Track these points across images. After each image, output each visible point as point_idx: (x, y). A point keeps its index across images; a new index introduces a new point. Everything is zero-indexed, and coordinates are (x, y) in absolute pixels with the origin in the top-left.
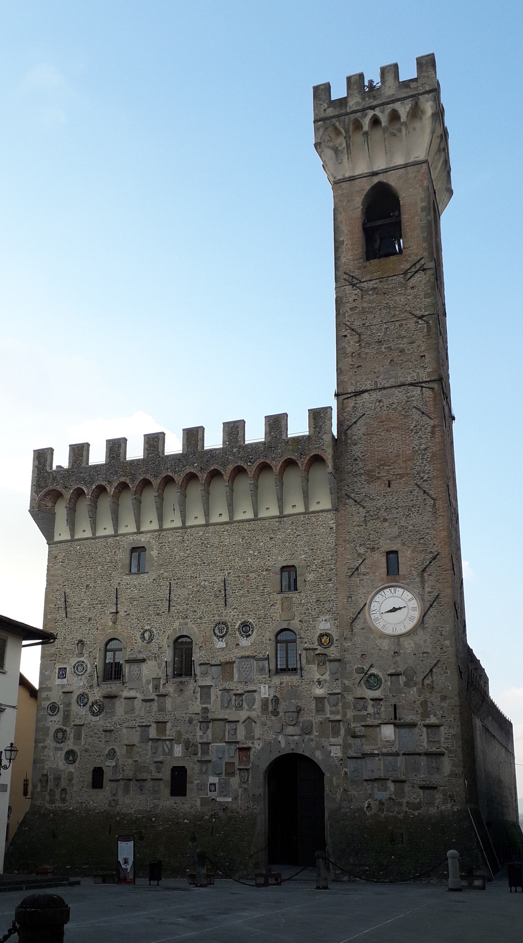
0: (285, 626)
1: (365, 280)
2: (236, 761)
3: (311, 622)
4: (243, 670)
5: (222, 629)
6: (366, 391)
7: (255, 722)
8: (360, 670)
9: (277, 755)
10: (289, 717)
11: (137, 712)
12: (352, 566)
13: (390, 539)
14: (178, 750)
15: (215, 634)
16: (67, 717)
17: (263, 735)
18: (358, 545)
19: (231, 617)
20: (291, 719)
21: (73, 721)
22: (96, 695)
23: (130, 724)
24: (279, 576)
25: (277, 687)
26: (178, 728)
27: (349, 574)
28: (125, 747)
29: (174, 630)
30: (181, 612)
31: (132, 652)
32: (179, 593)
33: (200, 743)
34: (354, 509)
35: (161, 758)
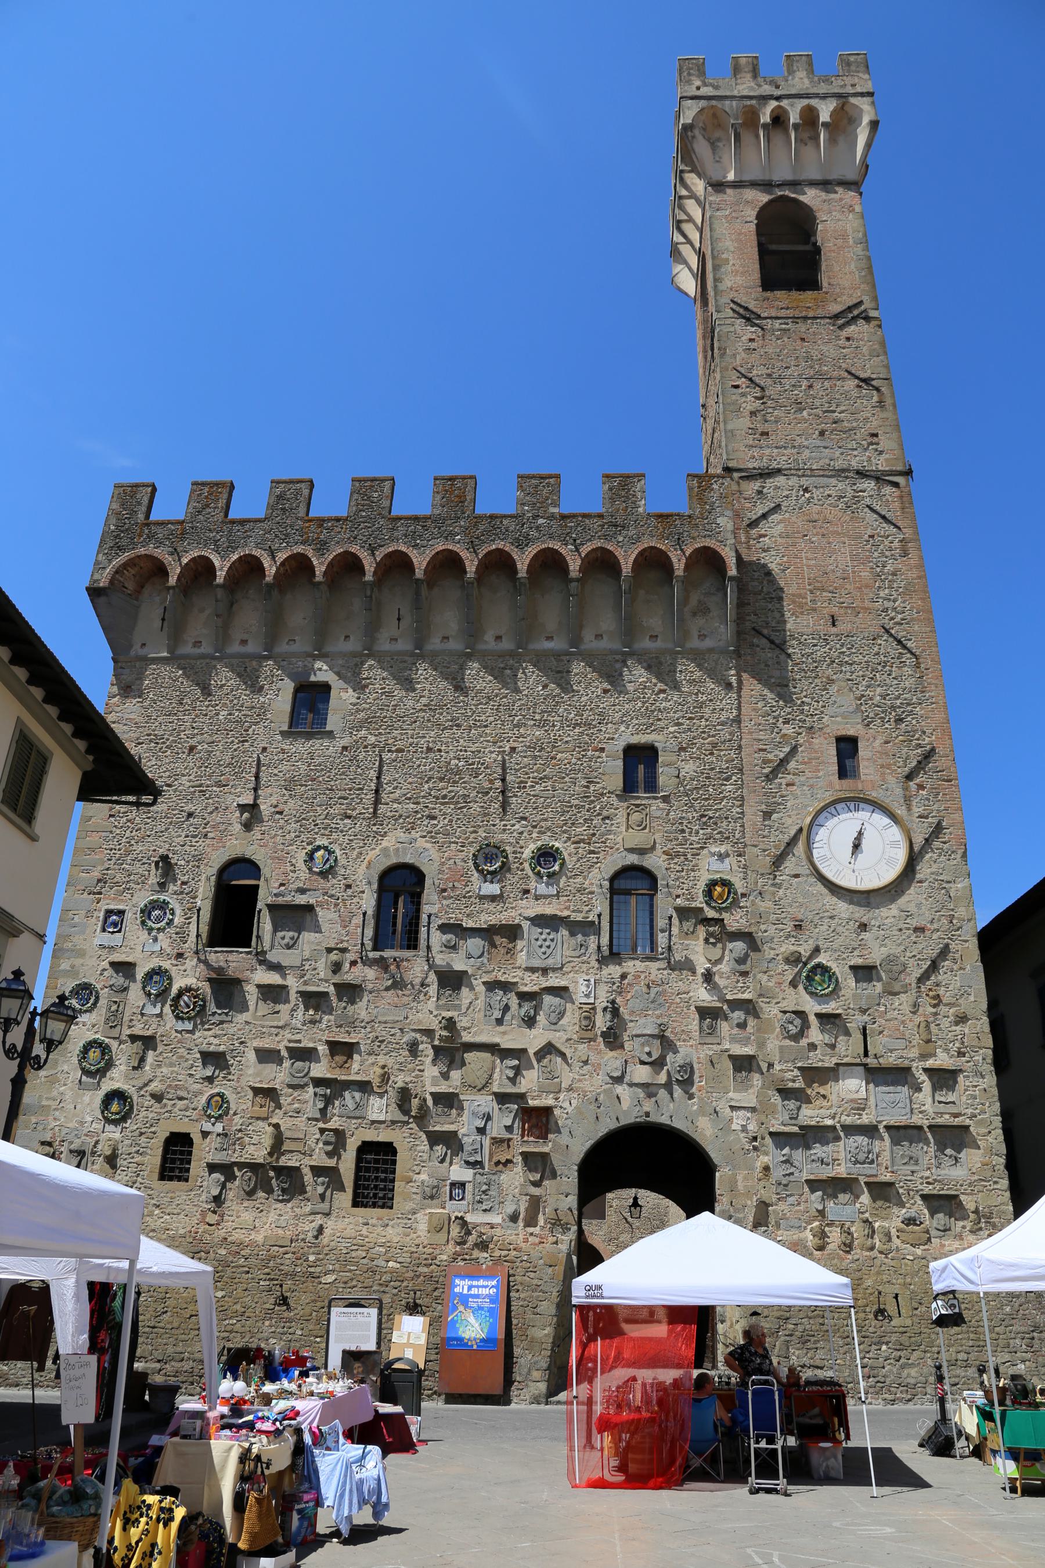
0: (633, 859)
1: (766, 315)
2: (516, 1136)
3: (689, 856)
4: (539, 943)
5: (492, 860)
7: (563, 1055)
8: (794, 959)
9: (612, 1125)
10: (643, 1045)
11: (284, 1017)
12: (770, 756)
14: (378, 1108)
15: (476, 866)
16: (114, 1019)
17: (580, 1080)
18: (781, 720)
20: (647, 1049)
21: (130, 1027)
22: (188, 976)
23: (266, 1043)
24: (620, 763)
25: (614, 983)
26: (381, 1060)
27: (767, 771)
28: (250, 1094)
29: (385, 849)
30: (401, 816)
31: (282, 888)
32: (399, 785)
33: (431, 1094)
34: (769, 655)
35: (334, 1123)
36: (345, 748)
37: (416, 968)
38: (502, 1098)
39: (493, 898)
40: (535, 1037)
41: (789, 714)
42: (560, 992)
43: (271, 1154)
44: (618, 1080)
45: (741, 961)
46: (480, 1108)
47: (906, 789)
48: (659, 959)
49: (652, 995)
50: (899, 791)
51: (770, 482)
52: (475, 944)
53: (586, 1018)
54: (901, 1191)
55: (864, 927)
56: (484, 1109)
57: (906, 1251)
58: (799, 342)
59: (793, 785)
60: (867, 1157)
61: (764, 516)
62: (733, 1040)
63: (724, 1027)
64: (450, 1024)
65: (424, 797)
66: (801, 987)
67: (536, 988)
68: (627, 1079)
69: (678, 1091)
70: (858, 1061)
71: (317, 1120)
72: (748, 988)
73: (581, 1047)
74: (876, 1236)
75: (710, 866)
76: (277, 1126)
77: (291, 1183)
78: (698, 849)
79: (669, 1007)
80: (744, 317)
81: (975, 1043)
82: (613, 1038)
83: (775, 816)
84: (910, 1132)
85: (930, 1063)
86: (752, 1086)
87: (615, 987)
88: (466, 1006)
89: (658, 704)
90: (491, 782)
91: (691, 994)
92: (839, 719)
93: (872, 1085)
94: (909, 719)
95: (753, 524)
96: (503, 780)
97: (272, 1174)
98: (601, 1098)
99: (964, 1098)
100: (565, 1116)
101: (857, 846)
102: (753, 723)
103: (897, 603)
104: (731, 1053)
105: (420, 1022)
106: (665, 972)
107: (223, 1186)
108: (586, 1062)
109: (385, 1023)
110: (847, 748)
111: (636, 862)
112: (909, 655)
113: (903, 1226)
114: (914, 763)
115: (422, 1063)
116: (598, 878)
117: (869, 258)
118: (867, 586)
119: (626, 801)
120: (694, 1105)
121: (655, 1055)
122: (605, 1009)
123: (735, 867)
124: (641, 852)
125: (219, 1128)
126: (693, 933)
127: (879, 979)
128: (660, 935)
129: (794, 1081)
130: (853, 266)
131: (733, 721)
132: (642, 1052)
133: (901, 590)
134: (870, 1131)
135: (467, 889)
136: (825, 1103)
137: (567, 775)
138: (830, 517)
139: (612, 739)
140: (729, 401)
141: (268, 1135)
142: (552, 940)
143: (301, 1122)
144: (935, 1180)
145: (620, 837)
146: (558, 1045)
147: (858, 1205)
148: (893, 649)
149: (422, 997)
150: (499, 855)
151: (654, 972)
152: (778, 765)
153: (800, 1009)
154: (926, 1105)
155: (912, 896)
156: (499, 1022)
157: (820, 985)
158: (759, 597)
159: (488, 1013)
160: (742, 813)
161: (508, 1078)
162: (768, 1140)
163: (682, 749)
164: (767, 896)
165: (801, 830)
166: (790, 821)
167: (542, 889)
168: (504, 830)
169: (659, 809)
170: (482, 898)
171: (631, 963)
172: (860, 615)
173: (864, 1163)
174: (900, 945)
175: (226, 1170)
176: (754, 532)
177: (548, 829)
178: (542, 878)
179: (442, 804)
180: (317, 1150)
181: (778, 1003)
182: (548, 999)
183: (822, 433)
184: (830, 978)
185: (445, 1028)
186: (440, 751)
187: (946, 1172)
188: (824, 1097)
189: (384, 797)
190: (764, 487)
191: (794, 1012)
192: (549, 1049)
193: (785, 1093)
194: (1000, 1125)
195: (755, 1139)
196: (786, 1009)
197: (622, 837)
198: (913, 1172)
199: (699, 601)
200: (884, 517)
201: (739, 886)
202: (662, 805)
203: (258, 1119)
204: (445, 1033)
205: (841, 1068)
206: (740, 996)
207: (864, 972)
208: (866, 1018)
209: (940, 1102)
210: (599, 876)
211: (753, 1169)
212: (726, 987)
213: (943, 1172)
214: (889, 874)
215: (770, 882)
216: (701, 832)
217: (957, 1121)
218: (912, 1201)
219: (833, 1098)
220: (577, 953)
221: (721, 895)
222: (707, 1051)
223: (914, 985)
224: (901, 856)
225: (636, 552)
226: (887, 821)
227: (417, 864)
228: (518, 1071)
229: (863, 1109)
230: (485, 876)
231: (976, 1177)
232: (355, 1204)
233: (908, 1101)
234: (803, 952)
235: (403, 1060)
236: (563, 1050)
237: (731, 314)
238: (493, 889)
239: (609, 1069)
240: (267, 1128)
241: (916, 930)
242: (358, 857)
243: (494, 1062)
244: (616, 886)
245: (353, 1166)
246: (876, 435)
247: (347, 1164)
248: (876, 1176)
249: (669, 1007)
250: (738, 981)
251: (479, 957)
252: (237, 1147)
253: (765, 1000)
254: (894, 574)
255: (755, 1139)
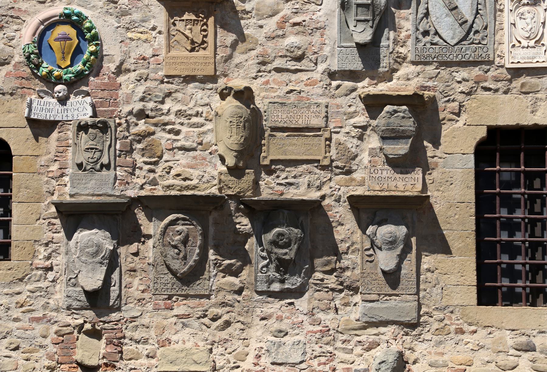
35: (405, 81)
43: (235, 172)
71: (353, 76)
76: (245, 96)
77: (298, 241)
97: (244, 223)
107: (113, 262)
125: (80, 109)
141: (223, 123)
143: (311, 82)
175: (118, 219)
180: (365, 158)
203: (189, 79)
232: (486, 296)
240: (216, 102)
245: (471, 195)
247: (451, 184)
252: (140, 160)
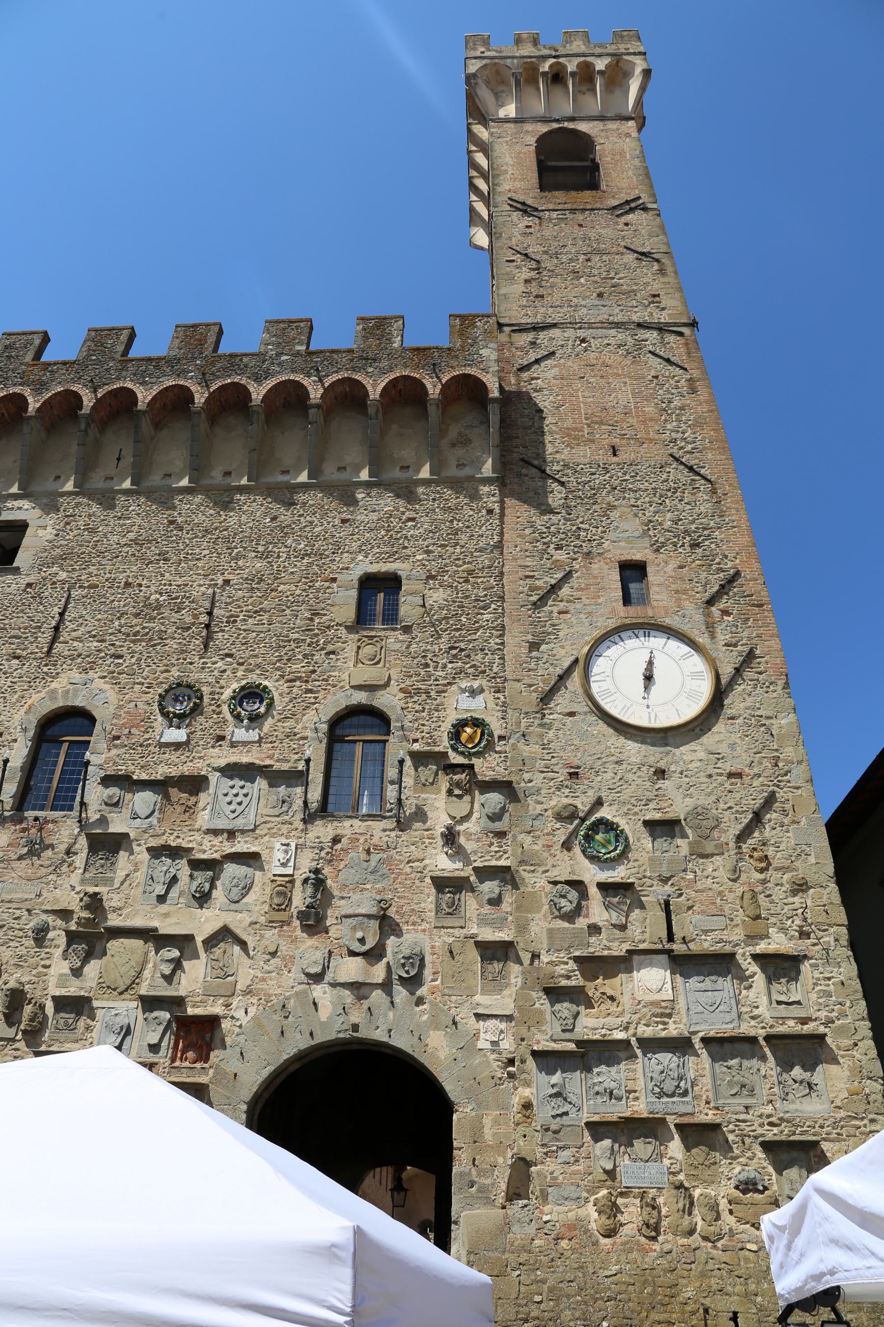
0: (360, 697)
3: (433, 694)
4: (228, 799)
5: (182, 702)
6: (554, 325)
7: (243, 944)
8: (568, 815)
10: (354, 929)
12: (539, 583)
13: (628, 540)
15: (162, 708)
17: (263, 980)
18: (552, 546)
19: (216, 673)
20: (359, 935)
24: (354, 593)
25: (322, 849)
27: (535, 598)
30: (79, 655)
32: (83, 621)
33: (54, 998)
36: (29, 585)
37: (65, 830)
38: (150, 1003)
39: (177, 746)
40: (207, 920)
41: (562, 539)
42: (251, 859)
44: (317, 978)
45: (495, 817)
46: (118, 1019)
47: (708, 615)
48: (385, 818)
49: (373, 863)
50: (699, 617)
51: (542, 335)
52: (144, 800)
53: (279, 894)
54: (731, 1137)
55: (661, 773)
56: (123, 1021)
57: (744, 1237)
58: (576, 227)
59: (566, 612)
60: (678, 1086)
61: (537, 361)
62: (483, 921)
63: (470, 904)
64: (95, 903)
65: (111, 634)
66: (577, 850)
67: (217, 856)
68: (329, 977)
69: (401, 993)
70: (660, 947)
72: (506, 853)
73: (269, 933)
74: (696, 1212)
75: (460, 704)
78: (445, 685)
79: (395, 879)
80: (520, 210)
81: (823, 918)
82: (313, 921)
83: (543, 647)
84: (738, 1046)
85: (762, 947)
86: (508, 985)
87: (323, 854)
88: (121, 879)
89: (404, 532)
90: (195, 617)
91: (426, 862)
92: (622, 544)
93: (679, 979)
94: (707, 543)
95: (523, 368)
96: (210, 614)
98: (291, 1004)
99: (813, 996)
100: (237, 1030)
101: (649, 678)
102: (518, 549)
103: (686, 435)
104: (479, 939)
105: (56, 900)
106: (393, 834)
108: (274, 954)
109: (10, 902)
110: (633, 572)
111: (364, 701)
112: (703, 482)
113: (738, 1194)
114: (716, 588)
115: (49, 956)
116: (314, 720)
117: (646, 168)
118: (651, 420)
119: (357, 633)
120: (423, 1014)
121: (370, 944)
122: (306, 881)
123: (491, 705)
124: (371, 688)
126: (432, 784)
127: (684, 836)
128: (390, 788)
129: (568, 977)
130: (630, 173)
131: (495, 547)
132: (352, 938)
133: (690, 423)
134: (680, 1045)
135: (147, 736)
136: (613, 1008)
137: (289, 608)
138: (610, 362)
139: (347, 569)
140: (503, 272)
142: (246, 795)
144: (781, 1119)
145: (347, 674)
146: (238, 931)
147: (667, 1162)
148: (684, 476)
149: (64, 868)
150: (193, 696)
151: (378, 834)
152: (549, 591)
153: (575, 878)
154: (759, 1005)
155: (720, 734)
156: (162, 899)
157: (604, 846)
158: (529, 431)
159: (149, 889)
160: (503, 644)
161: (164, 976)
162: (531, 1064)
163: (431, 577)
164: (532, 739)
165: (576, 661)
166: (563, 654)
167: (241, 734)
168: (203, 668)
169: (397, 641)
170: (162, 745)
171: (347, 823)
172: (645, 446)
173: (672, 1095)
174: (709, 795)
176: (525, 375)
177: (258, 666)
178: (242, 721)
179: (133, 642)
181: (547, 871)
182: (231, 870)
183: (600, 295)
184: (617, 836)
185: (87, 907)
186: (140, 585)
187: (797, 1106)
188: (612, 998)
189: (64, 636)
190: (537, 339)
191: (569, 883)
192: (224, 934)
193: (555, 994)
194: (871, 1034)
195: (511, 1062)
196: (557, 879)
197: (348, 673)
198: (747, 1108)
199: (460, 434)
200: (668, 361)
201: (497, 727)
202: (401, 638)
204: (85, 914)
205: (636, 958)
206: (494, 863)
207: (664, 828)
208: (668, 888)
209: (779, 1003)
210: (316, 719)
211: (506, 1107)
212: (475, 852)
213: (792, 1107)
214: (691, 708)
215: (537, 722)
216: (450, 666)
217: (807, 1029)
218: (749, 1154)
219: (626, 1001)
220: (277, 811)
221: (471, 738)
222: (446, 938)
223: (732, 845)
224: (704, 690)
225: (387, 380)
226: (685, 649)
227: (88, 708)
228: (177, 965)
229: (670, 1016)
230: (171, 721)
231: (843, 1113)
233: (733, 1001)
234: (580, 806)
235: (24, 952)
236: (244, 937)
237: (509, 208)
238: (178, 735)
239: (304, 963)
241: (730, 775)
242: (18, 701)
243: (146, 954)
244: (338, 732)
246: (658, 296)
248: (692, 1114)
249: (395, 879)
250: (492, 844)
251: (147, 818)
253: (528, 868)
254: (682, 408)
255: (511, 1062)
